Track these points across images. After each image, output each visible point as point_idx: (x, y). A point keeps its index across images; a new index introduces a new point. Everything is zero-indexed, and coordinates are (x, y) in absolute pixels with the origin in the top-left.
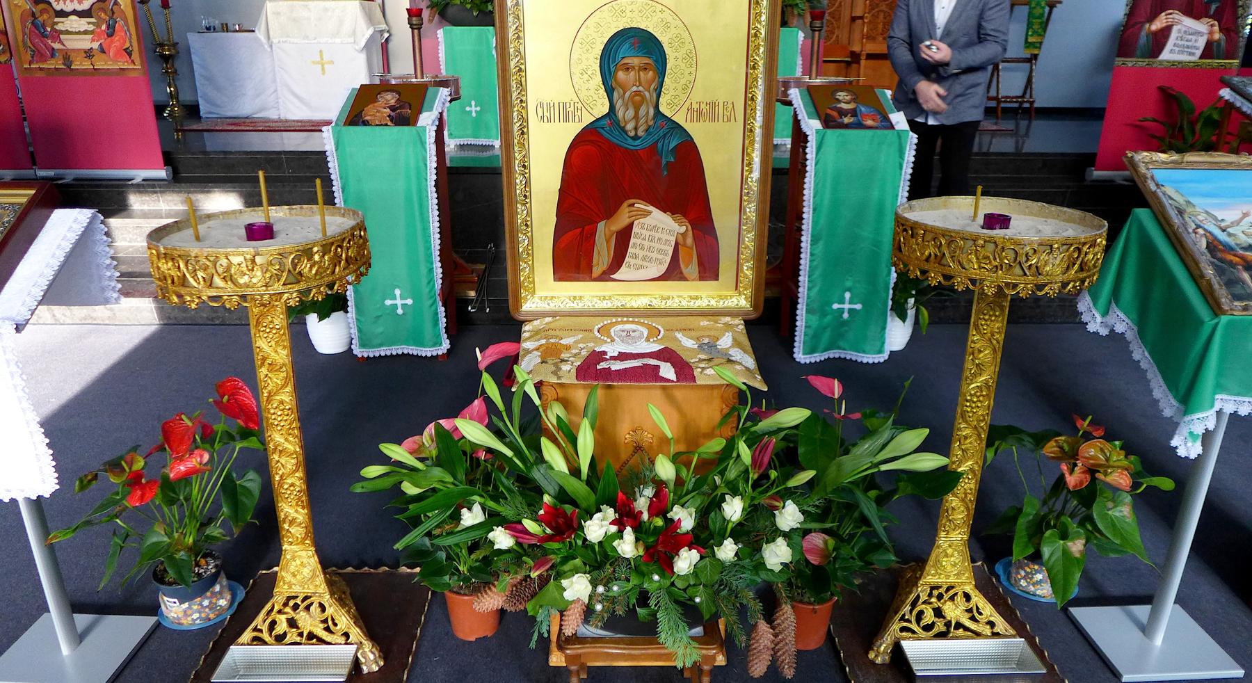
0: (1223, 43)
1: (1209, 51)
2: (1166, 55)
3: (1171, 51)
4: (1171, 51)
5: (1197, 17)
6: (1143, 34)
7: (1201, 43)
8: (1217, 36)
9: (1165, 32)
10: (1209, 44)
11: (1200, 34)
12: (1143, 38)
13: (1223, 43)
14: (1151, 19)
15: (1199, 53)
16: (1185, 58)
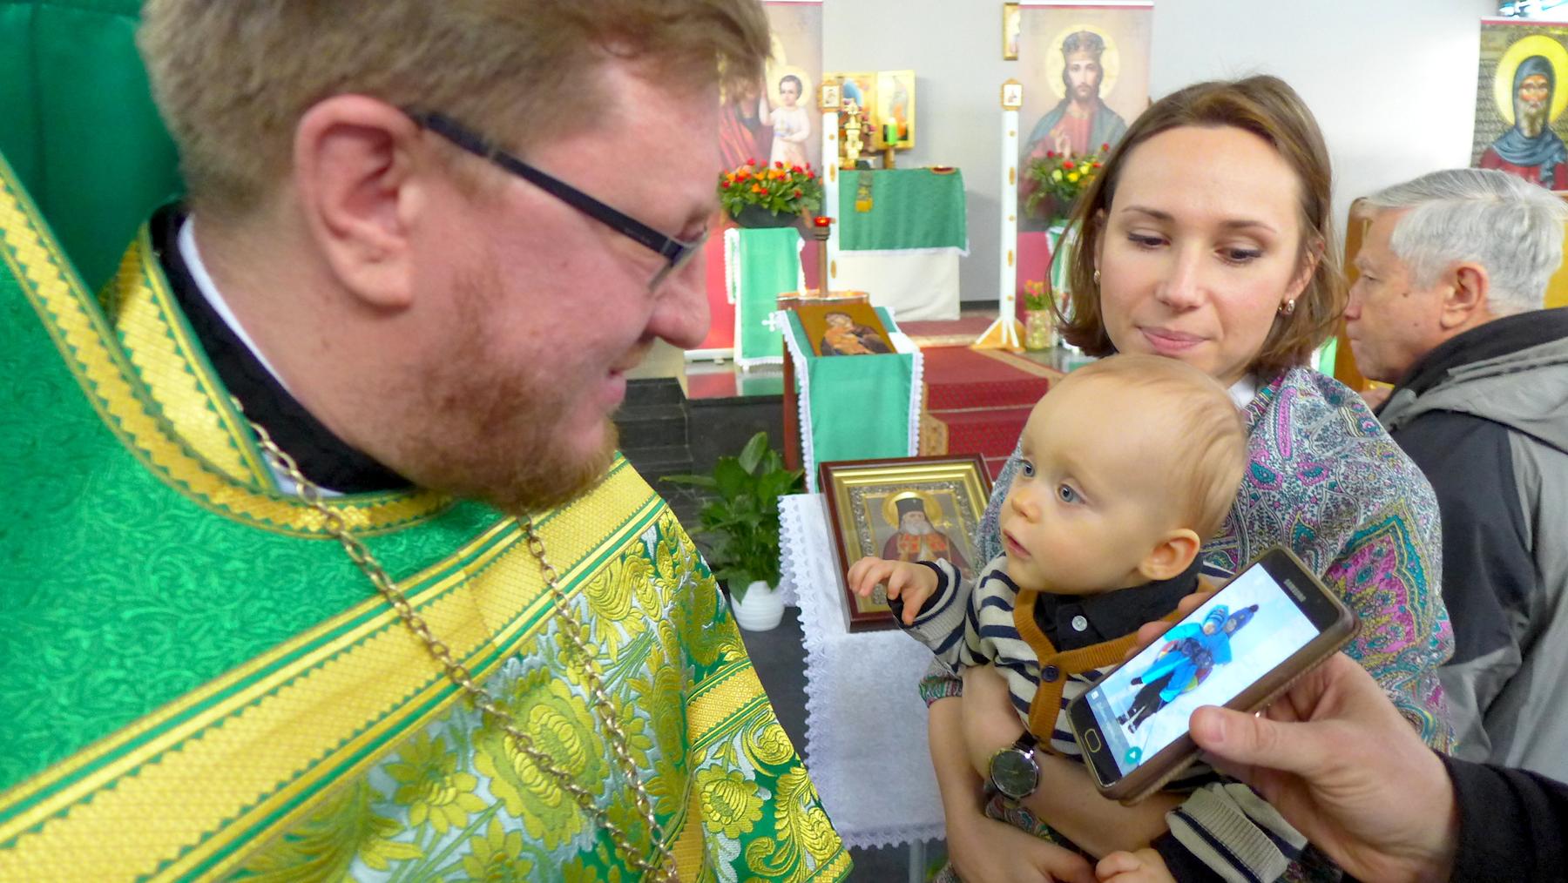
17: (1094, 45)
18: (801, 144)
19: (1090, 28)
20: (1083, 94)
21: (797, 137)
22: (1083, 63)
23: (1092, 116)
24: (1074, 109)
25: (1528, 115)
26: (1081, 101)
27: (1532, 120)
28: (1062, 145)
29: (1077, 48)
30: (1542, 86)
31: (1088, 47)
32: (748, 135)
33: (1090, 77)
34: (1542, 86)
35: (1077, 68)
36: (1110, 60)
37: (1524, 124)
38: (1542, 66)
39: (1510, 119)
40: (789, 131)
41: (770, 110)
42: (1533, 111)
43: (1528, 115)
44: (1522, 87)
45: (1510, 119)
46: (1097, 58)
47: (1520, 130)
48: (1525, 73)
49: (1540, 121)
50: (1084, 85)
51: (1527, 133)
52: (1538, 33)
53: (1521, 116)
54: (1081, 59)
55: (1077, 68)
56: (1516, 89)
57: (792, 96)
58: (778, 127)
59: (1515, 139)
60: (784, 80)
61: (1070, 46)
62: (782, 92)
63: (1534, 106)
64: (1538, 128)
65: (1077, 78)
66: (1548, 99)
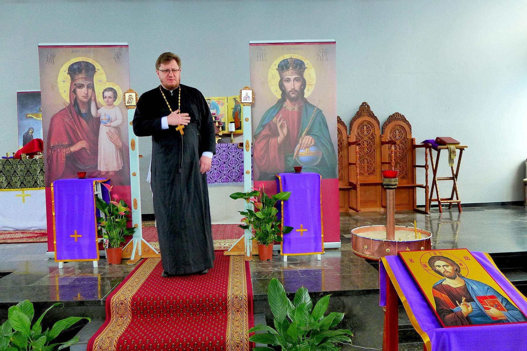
17: (299, 66)
18: (117, 128)
19: (295, 56)
20: (293, 96)
21: (114, 124)
22: (292, 78)
23: (300, 109)
24: (288, 105)
26: (292, 100)
28: (282, 126)
29: (287, 68)
31: (295, 68)
32: (84, 122)
33: (297, 85)
35: (288, 80)
36: (310, 74)
40: (109, 120)
41: (98, 108)
50: (294, 90)
54: (291, 74)
55: (288, 80)
57: (110, 100)
58: (103, 118)
60: (105, 90)
61: (283, 67)
62: (104, 97)
65: (289, 86)
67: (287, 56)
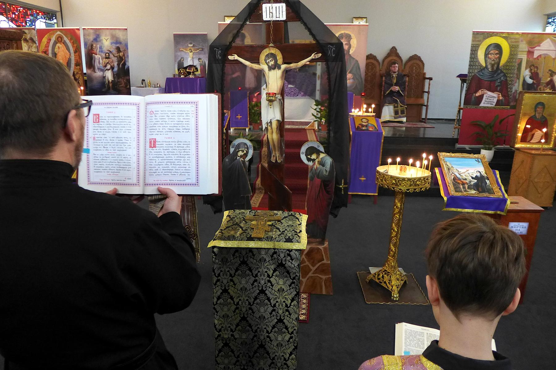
0: (503, 100)
1: (498, 103)
2: (482, 105)
3: (484, 103)
4: (484, 103)
5: (493, 92)
6: (473, 97)
7: (495, 100)
8: (501, 98)
9: (481, 97)
10: (498, 101)
11: (495, 97)
12: (473, 99)
13: (503, 100)
14: (476, 92)
15: (494, 104)
16: (489, 105)
19: (347, 32)
25: (490, 64)
27: (493, 66)
30: (497, 54)
34: (497, 54)
37: (489, 67)
38: (498, 47)
39: (484, 65)
42: (493, 62)
43: (490, 64)
44: (488, 54)
45: (484, 65)
46: (349, 41)
47: (488, 69)
48: (490, 50)
49: (496, 66)
51: (490, 70)
52: (496, 35)
53: (488, 64)
56: (486, 55)
59: (486, 72)
63: (494, 60)
64: (495, 68)
66: (500, 58)
67: (343, 32)
